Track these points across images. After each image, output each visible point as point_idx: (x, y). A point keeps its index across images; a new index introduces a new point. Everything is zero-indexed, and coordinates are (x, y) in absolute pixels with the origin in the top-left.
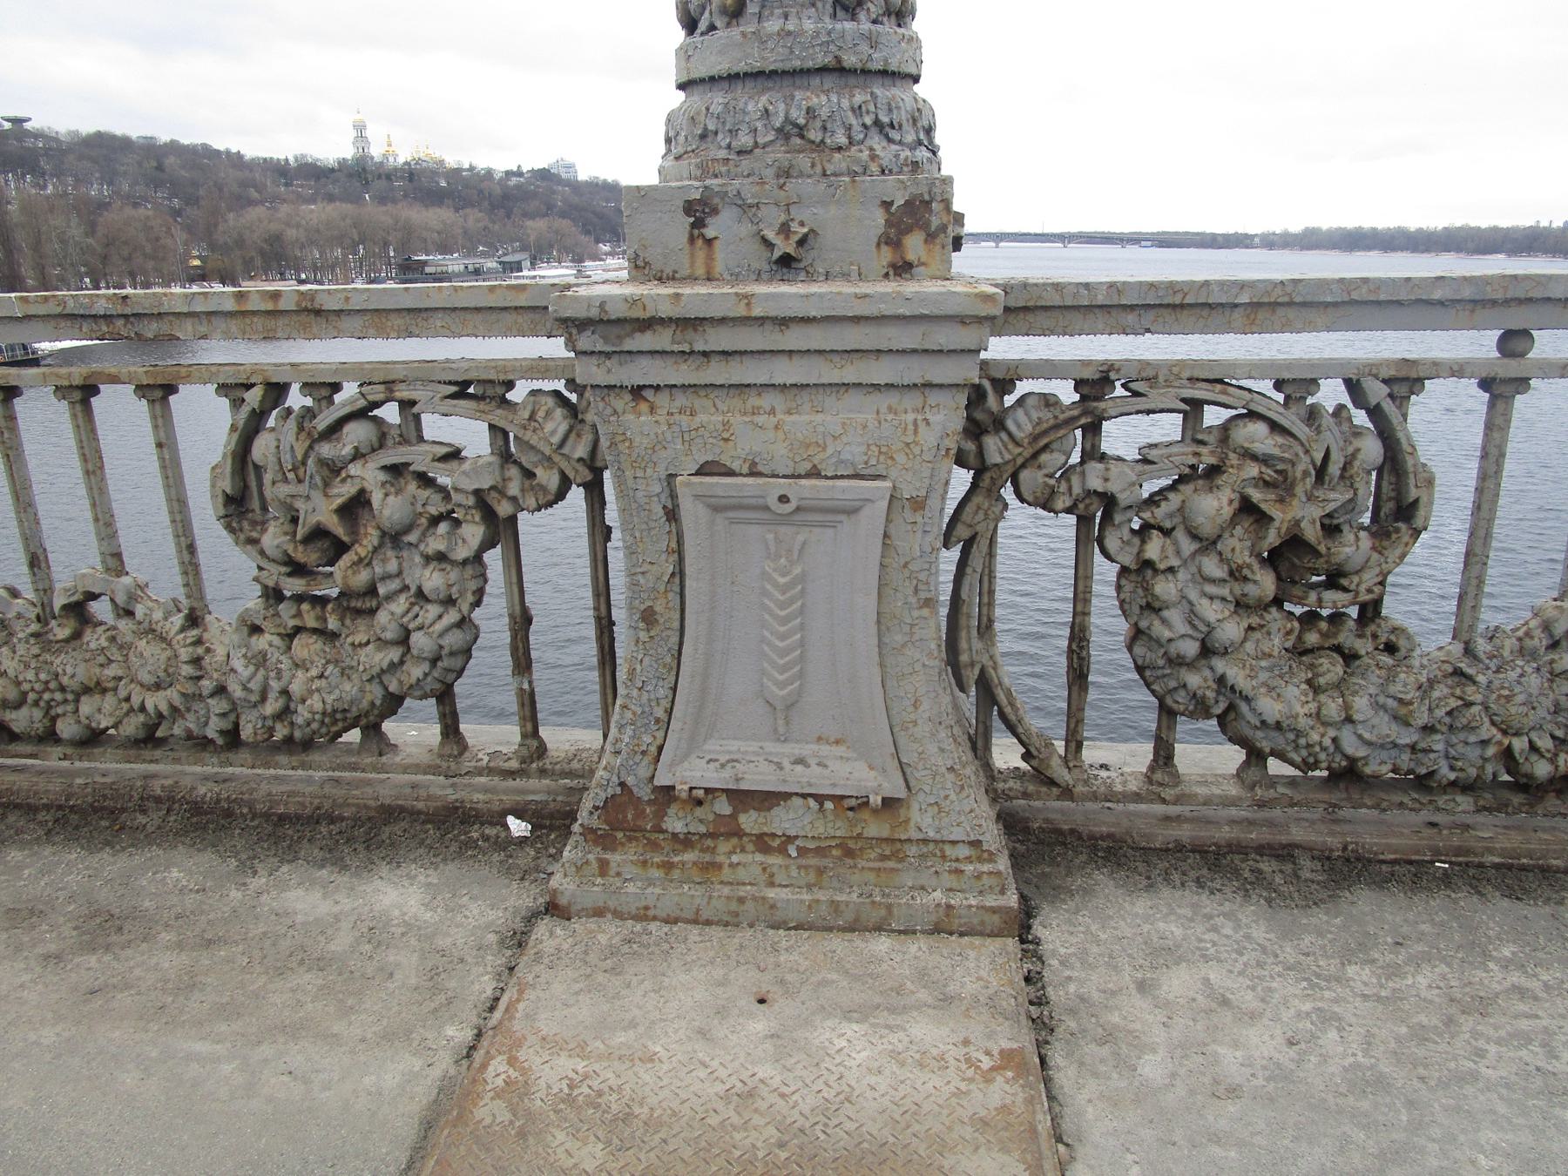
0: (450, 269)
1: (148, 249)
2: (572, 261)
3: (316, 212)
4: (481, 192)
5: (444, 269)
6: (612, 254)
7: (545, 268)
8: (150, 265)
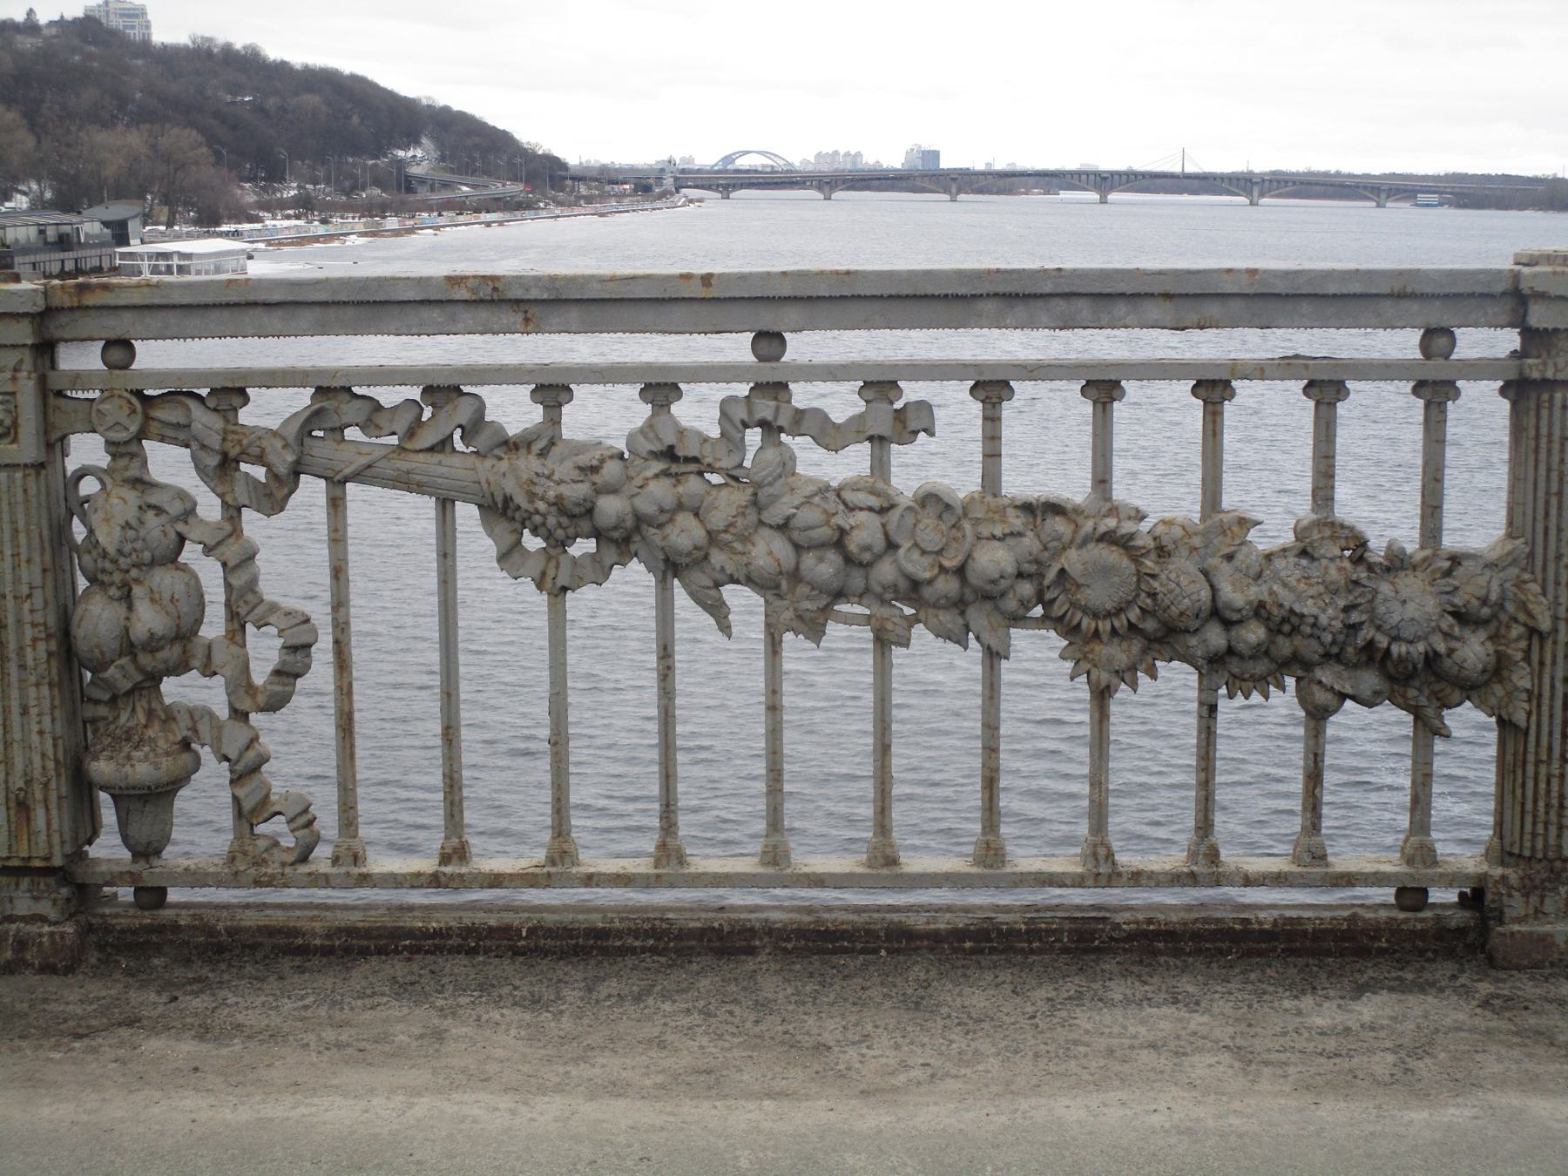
2: (197, 222)
6: (275, 207)
7: (164, 238)
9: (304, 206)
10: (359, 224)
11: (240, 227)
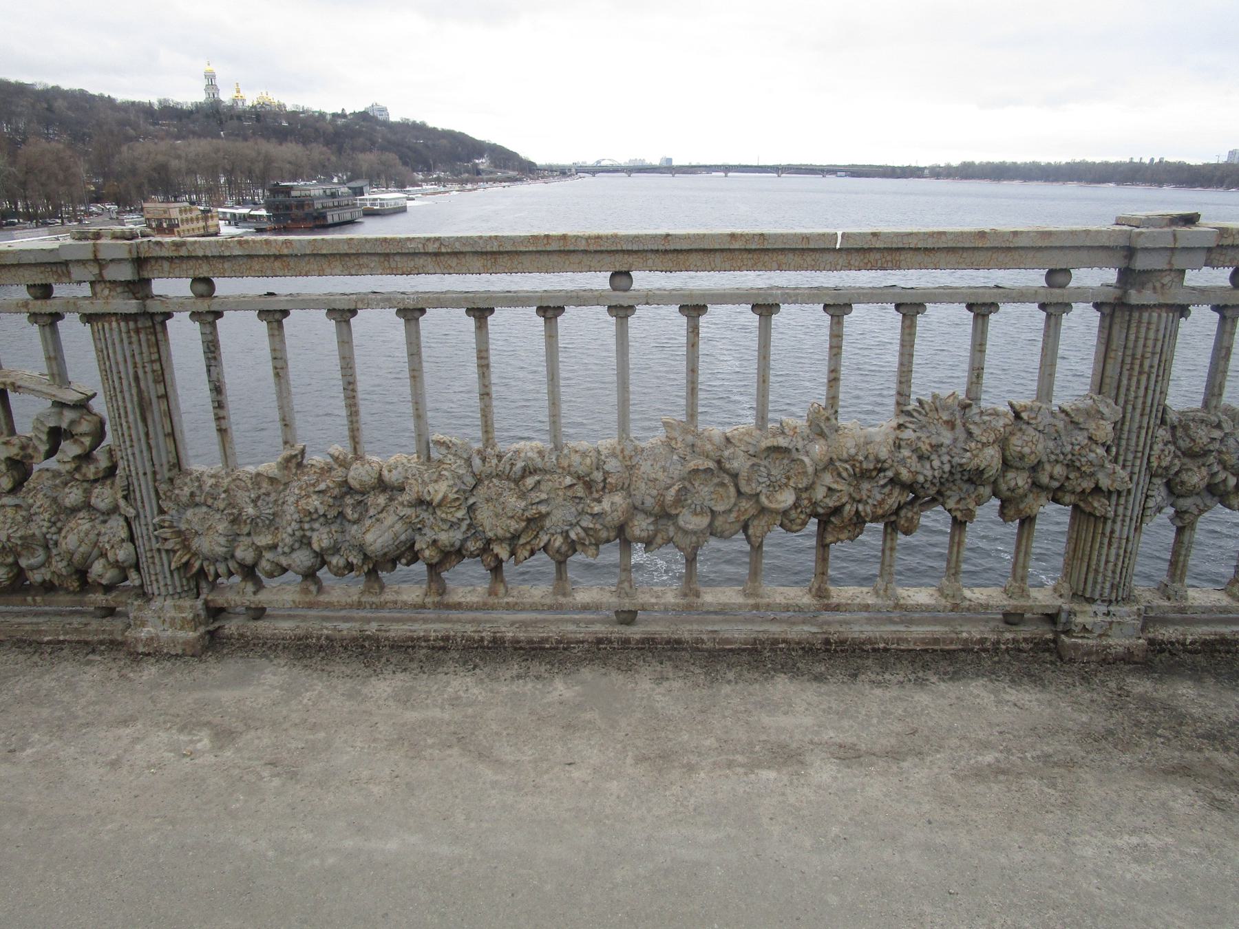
0: (312, 194)
1: (61, 176)
3: (198, 147)
4: (316, 130)
5: (308, 193)
6: (426, 181)
8: (62, 190)
9: (438, 181)
10: (457, 187)
11: (410, 189)
